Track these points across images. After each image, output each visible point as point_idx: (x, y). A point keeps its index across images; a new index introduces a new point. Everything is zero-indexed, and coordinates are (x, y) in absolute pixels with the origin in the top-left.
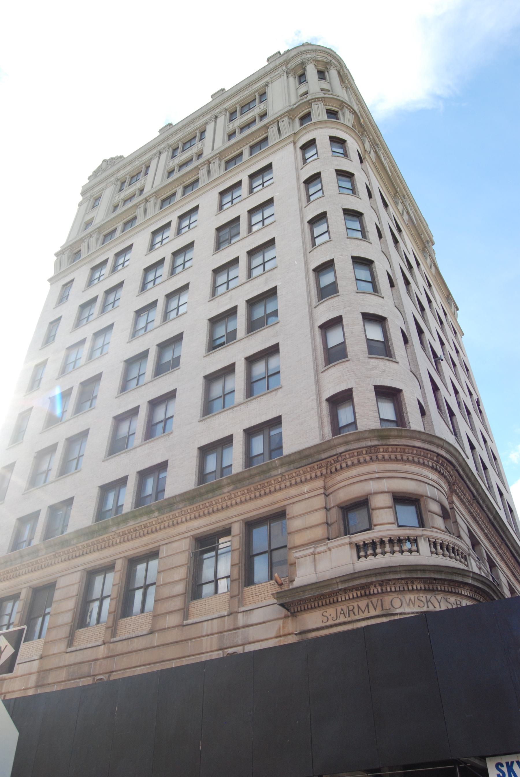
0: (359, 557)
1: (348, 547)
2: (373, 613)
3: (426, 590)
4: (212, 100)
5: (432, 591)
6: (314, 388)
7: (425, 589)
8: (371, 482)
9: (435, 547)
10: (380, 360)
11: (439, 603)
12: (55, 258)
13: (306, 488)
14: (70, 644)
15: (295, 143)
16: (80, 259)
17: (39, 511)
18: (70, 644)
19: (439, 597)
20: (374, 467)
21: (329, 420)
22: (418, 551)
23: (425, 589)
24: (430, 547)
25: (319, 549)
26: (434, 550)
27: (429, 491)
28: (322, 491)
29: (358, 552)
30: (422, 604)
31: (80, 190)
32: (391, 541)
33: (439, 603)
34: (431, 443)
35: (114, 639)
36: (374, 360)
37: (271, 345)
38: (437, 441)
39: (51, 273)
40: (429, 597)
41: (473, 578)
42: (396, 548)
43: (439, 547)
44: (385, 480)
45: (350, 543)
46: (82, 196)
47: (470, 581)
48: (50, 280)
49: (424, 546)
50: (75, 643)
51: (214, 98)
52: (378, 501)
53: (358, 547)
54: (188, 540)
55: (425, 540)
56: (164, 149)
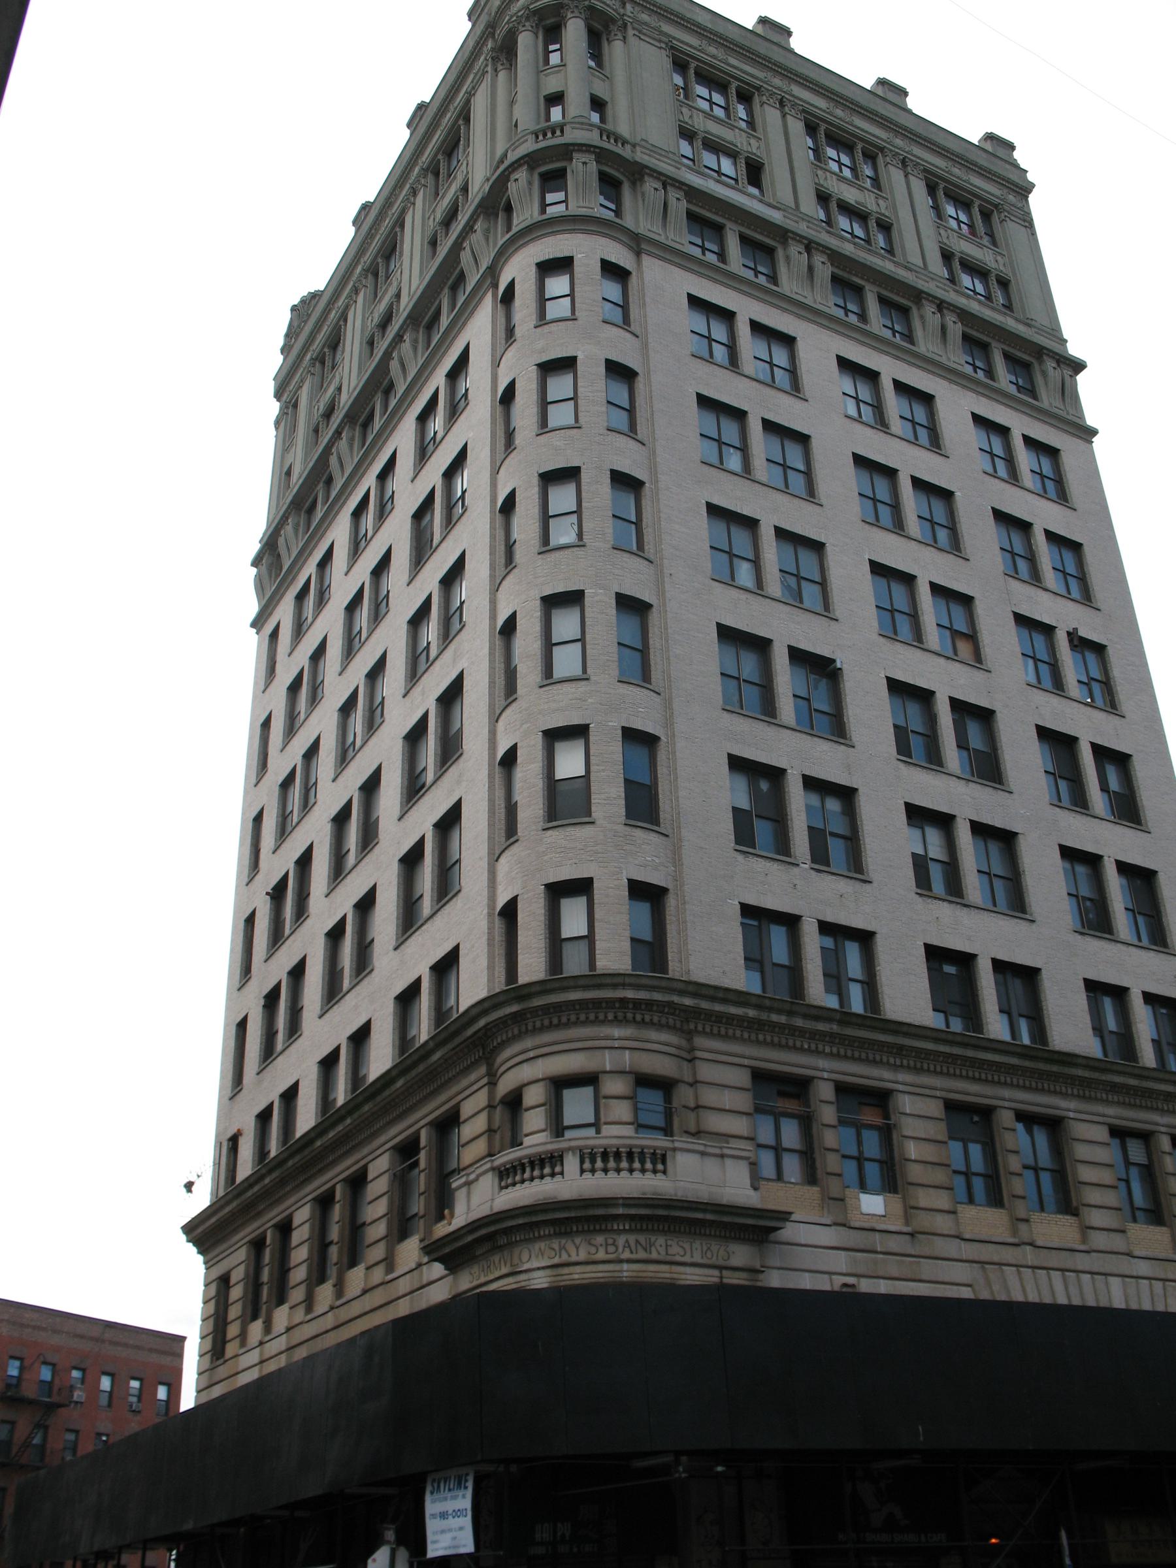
0: (502, 1188)
1: (490, 1175)
2: (504, 1271)
3: (558, 1235)
4: (473, 26)
5: (567, 1234)
6: (486, 893)
7: (555, 1234)
8: (525, 1065)
9: (593, 1161)
10: (560, 829)
11: (577, 1248)
12: (254, 570)
13: (473, 1077)
14: (309, 1309)
15: (495, 286)
16: (284, 571)
17: (272, 1103)
18: (309, 1309)
19: (578, 1240)
20: (528, 1043)
21: (503, 952)
22: (562, 1173)
23: (555, 1234)
24: (582, 1162)
25: (472, 1177)
26: (587, 1165)
27: (607, 1061)
28: (485, 1080)
29: (501, 1179)
30: (553, 1253)
31: (270, 387)
32: (532, 1164)
33: (577, 1248)
34: (599, 986)
35: (344, 1300)
36: (550, 832)
37: (412, 844)
38: (608, 981)
39: (251, 606)
40: (563, 1241)
41: (624, 1205)
42: (547, 1170)
43: (599, 1160)
44: (540, 1060)
45: (493, 1169)
46: (278, 400)
47: (621, 1211)
48: (254, 624)
49: (571, 1163)
50: (315, 1309)
51: (474, 18)
52: (534, 1096)
53: (500, 1172)
54: (387, 1154)
55: (574, 1154)
56: (417, 181)
